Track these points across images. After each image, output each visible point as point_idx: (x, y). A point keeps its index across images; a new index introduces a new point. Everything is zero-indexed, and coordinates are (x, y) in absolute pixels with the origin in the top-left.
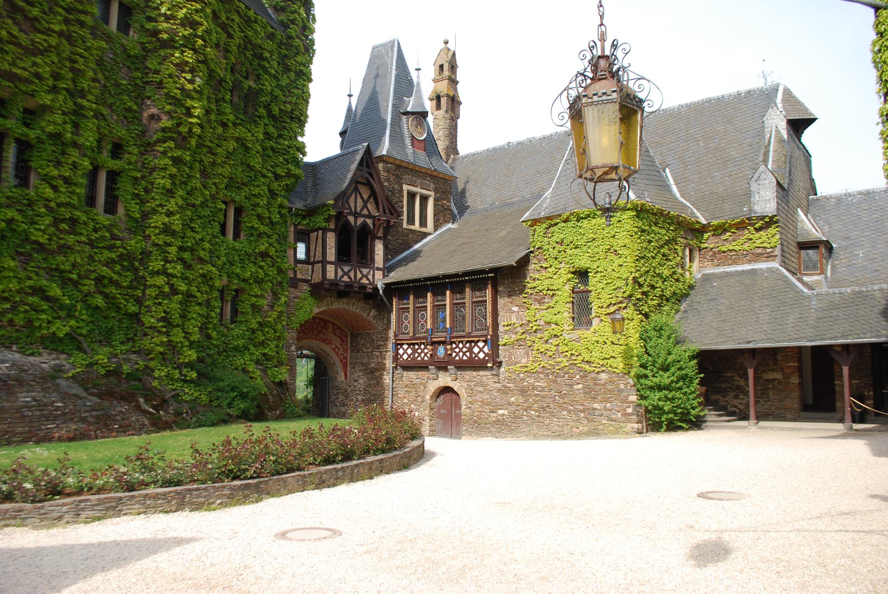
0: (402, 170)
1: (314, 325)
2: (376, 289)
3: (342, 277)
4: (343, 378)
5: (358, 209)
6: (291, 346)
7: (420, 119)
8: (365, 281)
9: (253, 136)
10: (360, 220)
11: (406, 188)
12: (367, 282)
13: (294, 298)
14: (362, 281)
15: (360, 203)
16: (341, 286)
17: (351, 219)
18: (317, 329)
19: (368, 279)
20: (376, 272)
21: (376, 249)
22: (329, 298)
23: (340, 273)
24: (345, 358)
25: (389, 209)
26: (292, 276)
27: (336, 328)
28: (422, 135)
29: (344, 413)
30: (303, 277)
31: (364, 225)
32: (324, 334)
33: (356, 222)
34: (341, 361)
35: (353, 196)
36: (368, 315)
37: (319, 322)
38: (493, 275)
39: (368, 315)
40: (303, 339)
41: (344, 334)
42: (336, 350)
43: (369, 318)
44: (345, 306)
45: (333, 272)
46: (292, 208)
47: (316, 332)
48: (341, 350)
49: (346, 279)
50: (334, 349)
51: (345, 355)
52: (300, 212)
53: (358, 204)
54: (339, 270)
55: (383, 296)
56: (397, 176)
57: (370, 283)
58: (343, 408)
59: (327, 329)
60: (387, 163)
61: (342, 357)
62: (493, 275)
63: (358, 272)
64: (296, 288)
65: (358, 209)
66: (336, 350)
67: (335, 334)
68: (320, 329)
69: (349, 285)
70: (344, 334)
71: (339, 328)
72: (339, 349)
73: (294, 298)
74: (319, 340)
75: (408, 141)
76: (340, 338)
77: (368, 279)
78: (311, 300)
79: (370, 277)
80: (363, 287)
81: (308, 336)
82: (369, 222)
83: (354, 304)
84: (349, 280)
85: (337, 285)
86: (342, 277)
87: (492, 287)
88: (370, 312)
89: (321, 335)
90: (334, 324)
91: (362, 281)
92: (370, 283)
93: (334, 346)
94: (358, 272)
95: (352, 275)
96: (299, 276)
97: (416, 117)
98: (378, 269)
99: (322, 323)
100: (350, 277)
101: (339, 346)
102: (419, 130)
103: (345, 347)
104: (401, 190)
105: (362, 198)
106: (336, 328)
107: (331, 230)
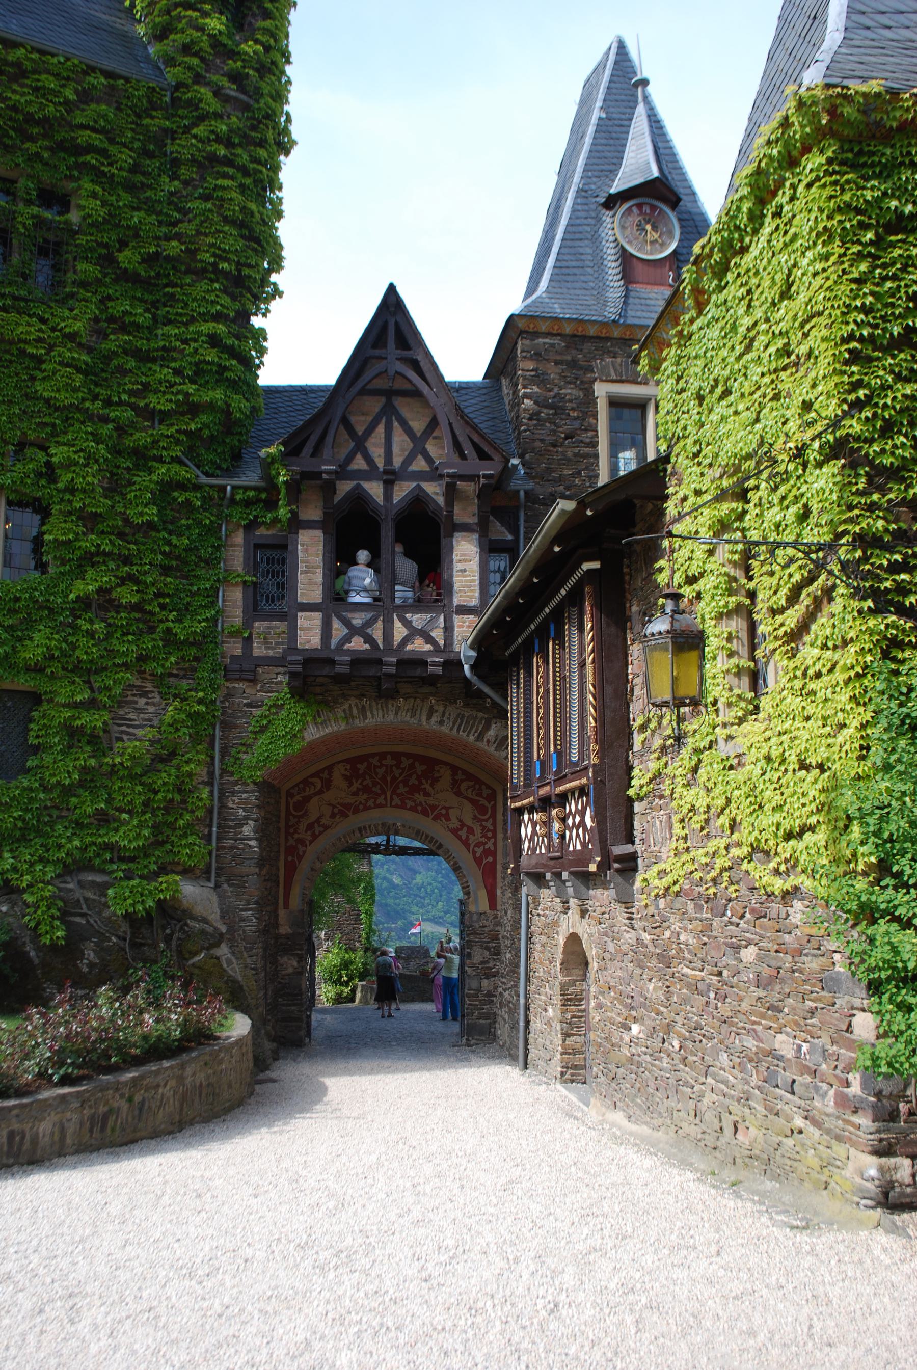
0: (587, 346)
1: (397, 772)
2: (453, 665)
3: (347, 639)
4: (484, 905)
5: (397, 462)
6: (241, 826)
7: (653, 208)
8: (419, 645)
9: (53, 329)
10: (402, 491)
11: (601, 390)
12: (428, 647)
13: (249, 705)
14: (409, 647)
15: (400, 443)
16: (342, 664)
17: (375, 490)
18: (405, 782)
19: (429, 640)
20: (457, 619)
21: (455, 558)
22: (353, 701)
23: (338, 630)
24: (493, 853)
25: (475, 446)
26: (238, 652)
27: (460, 776)
28: (663, 245)
29: (490, 994)
30: (271, 653)
31: (418, 501)
32: (427, 794)
33: (388, 496)
34: (478, 861)
35: (381, 429)
36: (480, 738)
37: (412, 766)
38: (596, 565)
39: (480, 738)
40: (366, 808)
41: (486, 792)
42: (463, 833)
43: (483, 745)
44: (405, 717)
45: (318, 631)
46: (225, 487)
47: (402, 789)
48: (478, 831)
49: (357, 644)
50: (455, 832)
51: (490, 845)
52: (251, 493)
53: (396, 449)
54: (336, 624)
55: (475, 680)
56: (573, 364)
57: (437, 650)
58: (485, 983)
59: (436, 780)
60: (536, 334)
61: (479, 851)
62: (596, 565)
63: (398, 624)
64: (253, 681)
65: (397, 462)
66: (463, 833)
67: (458, 794)
68: (413, 781)
69: (358, 661)
70: (486, 792)
71: (469, 777)
72: (471, 831)
73: (249, 705)
74: (413, 809)
75: (612, 268)
76: (473, 802)
77: (429, 640)
78: (294, 711)
79: (438, 634)
80: (420, 662)
81: (381, 800)
82: (433, 490)
83: (431, 712)
84: (367, 646)
85: (332, 662)
86: (347, 639)
87: (598, 606)
88: (487, 727)
89: (419, 798)
90: (454, 769)
91: (409, 647)
92: (437, 650)
93: (454, 824)
94: (398, 624)
95: (377, 633)
96: (258, 650)
97: (639, 206)
98: (464, 610)
99: (420, 768)
100: (369, 639)
101: (469, 822)
102: (652, 235)
103: (489, 825)
104: (589, 400)
105: (409, 431)
106: (460, 776)
107: (310, 525)
